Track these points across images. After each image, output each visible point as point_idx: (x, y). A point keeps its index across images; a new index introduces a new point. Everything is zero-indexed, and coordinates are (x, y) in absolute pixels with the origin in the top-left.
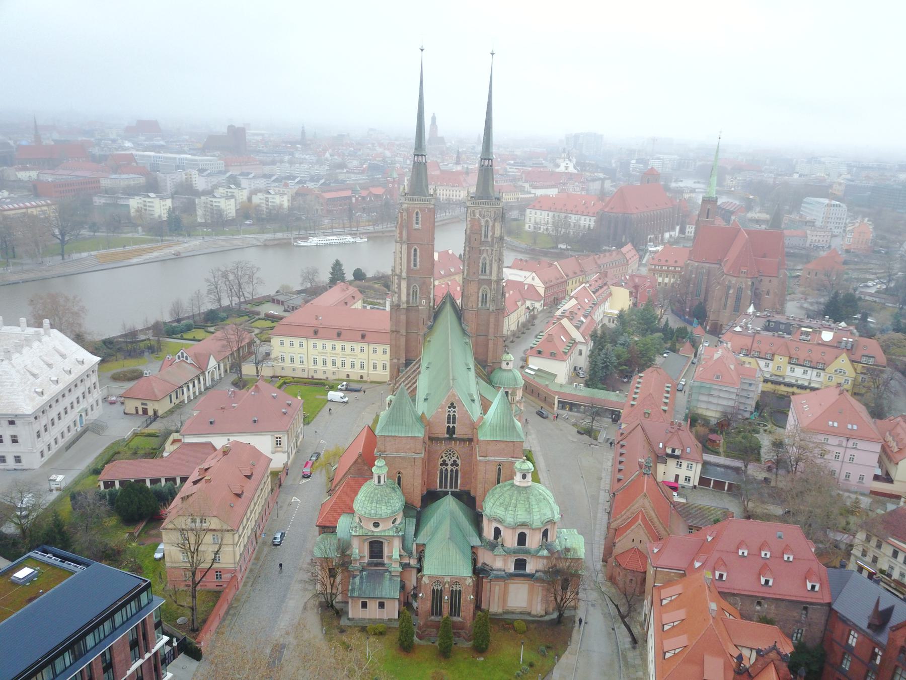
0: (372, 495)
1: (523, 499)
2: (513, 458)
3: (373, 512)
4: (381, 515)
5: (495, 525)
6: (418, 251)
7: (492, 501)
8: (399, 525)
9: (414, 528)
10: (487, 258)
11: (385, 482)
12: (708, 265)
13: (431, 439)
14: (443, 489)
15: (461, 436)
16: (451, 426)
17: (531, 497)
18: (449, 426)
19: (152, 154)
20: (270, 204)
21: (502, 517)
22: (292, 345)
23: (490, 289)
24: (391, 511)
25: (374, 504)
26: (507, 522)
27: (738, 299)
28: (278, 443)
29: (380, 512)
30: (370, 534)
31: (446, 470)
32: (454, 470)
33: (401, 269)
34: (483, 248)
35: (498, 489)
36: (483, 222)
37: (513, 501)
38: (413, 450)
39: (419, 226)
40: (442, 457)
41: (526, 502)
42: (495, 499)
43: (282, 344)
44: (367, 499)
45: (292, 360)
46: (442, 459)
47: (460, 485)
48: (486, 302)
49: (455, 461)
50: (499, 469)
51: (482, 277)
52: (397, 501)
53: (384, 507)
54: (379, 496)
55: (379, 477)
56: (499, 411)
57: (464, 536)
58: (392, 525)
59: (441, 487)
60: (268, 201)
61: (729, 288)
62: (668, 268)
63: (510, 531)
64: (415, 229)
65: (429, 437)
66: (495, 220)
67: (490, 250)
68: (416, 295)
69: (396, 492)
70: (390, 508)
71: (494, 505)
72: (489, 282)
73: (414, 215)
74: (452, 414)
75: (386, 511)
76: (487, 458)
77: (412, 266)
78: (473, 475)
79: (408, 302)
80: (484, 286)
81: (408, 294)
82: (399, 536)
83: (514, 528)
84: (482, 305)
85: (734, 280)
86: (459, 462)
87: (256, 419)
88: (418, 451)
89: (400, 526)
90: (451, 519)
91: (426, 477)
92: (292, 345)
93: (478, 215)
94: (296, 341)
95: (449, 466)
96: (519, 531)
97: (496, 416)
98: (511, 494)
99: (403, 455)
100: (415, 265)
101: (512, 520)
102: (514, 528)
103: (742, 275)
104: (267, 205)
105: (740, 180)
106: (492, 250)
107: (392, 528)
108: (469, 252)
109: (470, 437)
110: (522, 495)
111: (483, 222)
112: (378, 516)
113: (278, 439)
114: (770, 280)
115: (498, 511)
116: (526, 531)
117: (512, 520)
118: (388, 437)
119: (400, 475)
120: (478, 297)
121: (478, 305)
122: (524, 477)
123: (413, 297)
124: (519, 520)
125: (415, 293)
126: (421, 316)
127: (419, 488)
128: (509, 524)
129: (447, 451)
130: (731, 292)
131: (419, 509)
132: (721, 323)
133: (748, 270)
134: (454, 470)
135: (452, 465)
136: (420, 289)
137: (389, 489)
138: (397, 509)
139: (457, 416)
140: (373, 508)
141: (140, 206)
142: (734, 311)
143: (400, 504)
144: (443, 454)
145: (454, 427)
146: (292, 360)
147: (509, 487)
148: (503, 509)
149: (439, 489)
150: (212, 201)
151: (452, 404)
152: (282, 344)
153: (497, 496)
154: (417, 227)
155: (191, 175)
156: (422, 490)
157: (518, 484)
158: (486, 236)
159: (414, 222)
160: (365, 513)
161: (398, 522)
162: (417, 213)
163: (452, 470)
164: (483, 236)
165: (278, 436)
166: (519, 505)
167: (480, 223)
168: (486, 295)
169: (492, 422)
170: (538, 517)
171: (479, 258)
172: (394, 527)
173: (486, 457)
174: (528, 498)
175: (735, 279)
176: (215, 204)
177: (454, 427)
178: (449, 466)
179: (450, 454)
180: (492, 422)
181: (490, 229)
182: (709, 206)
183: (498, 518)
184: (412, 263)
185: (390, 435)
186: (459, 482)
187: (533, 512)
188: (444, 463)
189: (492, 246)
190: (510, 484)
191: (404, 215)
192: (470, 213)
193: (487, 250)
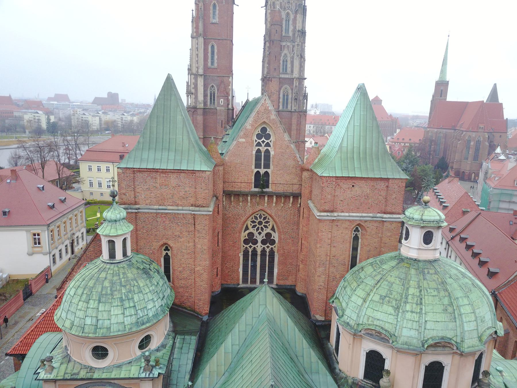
0: (91, 284)
1: (433, 285)
2: (385, 213)
3: (88, 321)
4: (109, 329)
5: (369, 345)
6: (216, 47)
7: (360, 292)
8: (158, 350)
9: (191, 355)
10: (288, 55)
11: (125, 254)
12: (445, 130)
13: (228, 194)
14: (249, 285)
15: (280, 189)
16: (262, 171)
17: (449, 281)
18: (258, 172)
19: (56, 103)
20: (124, 121)
21: (387, 327)
22: (99, 170)
23: (292, 90)
24: (134, 319)
25: (92, 304)
26: (401, 340)
27: (477, 150)
28: (37, 242)
29: (107, 323)
30: (83, 374)
31: (254, 252)
32: (268, 250)
33: (197, 68)
34: (284, 44)
35: (369, 270)
36: (284, 16)
37: (411, 291)
38: (192, 201)
39: (216, 20)
40: (247, 228)
41: (442, 293)
42: (368, 289)
43: (90, 169)
44: (80, 291)
45: (100, 185)
46: (247, 232)
47: (278, 274)
48: (287, 103)
49: (268, 235)
50: (356, 238)
51: (282, 76)
52: (150, 296)
53: (116, 311)
54: (107, 284)
55: (111, 243)
56: (357, 124)
57: (299, 373)
58: (139, 353)
59: (245, 281)
60: (122, 120)
61: (469, 141)
62: (405, 144)
63: (409, 361)
64: (213, 23)
65: (224, 192)
66: (296, 12)
67: (291, 46)
68: (214, 97)
69: (150, 277)
70: (133, 312)
71: (365, 301)
72: (291, 81)
73: (211, 8)
74: (263, 149)
75: (120, 319)
76: (335, 214)
77: (209, 64)
78: (301, 257)
79: (205, 103)
80: (285, 86)
81: (205, 96)
82: (153, 379)
83: (418, 354)
84: (283, 107)
85: (474, 135)
86: (275, 236)
87: (7, 210)
88: (200, 202)
89: (159, 354)
90: (271, 336)
91: (219, 261)
92: (99, 170)
93: (278, 7)
94: (103, 166)
95: (259, 244)
96: (428, 359)
97: (351, 133)
98: (403, 276)
99: (171, 209)
100: (212, 63)
101: (413, 333)
102: (418, 354)
103: (481, 130)
104: (122, 122)
105: (418, 123)
106: (293, 46)
107: (138, 360)
108: (269, 47)
109: (295, 189)
110: (428, 277)
111: (284, 16)
112: (100, 333)
113: (37, 237)
114: (500, 136)
115: (378, 315)
116: (446, 360)
117: (413, 333)
118: (140, 170)
119: (169, 253)
120: (279, 98)
121: (279, 106)
122: (428, 238)
123: (211, 99)
124: (429, 334)
125: (212, 96)
126: (218, 118)
127: (205, 276)
128: (406, 344)
129: (256, 218)
130: (472, 143)
131: (205, 318)
132: (463, 171)
133: (484, 126)
134: (268, 250)
135: (264, 242)
136: (218, 90)
137: (135, 271)
138: (151, 315)
139: (272, 153)
140: (90, 311)
141: (31, 119)
142: (474, 160)
143: (158, 304)
144: (249, 222)
145: (267, 173)
146: (100, 185)
147: (393, 263)
148: (391, 310)
149: (242, 285)
150: (83, 117)
151: (264, 130)
152: (90, 169)
153: (371, 282)
154: (214, 21)
155: (76, 111)
156: (212, 286)
157: (413, 254)
158: (287, 30)
159: (211, 15)
160: (72, 324)
161: (154, 345)
162: (214, 5)
163: (263, 251)
164: (284, 31)
165: (36, 232)
166: (427, 300)
167: (281, 16)
168: (287, 96)
169: (345, 144)
170: (472, 326)
171: (280, 54)
172: (143, 355)
173: (332, 211)
174: (443, 283)
175: (474, 133)
176: (84, 119)
177: (267, 173)
178: (259, 244)
179: (260, 223)
180: (345, 144)
181: (291, 22)
182: (442, 88)
183: (378, 329)
184: (210, 60)
185: (144, 166)
186: (276, 271)
187: (460, 315)
188: (251, 239)
189: (293, 41)
190: (392, 258)
191: (200, 5)
192: (270, 5)
193: (288, 46)
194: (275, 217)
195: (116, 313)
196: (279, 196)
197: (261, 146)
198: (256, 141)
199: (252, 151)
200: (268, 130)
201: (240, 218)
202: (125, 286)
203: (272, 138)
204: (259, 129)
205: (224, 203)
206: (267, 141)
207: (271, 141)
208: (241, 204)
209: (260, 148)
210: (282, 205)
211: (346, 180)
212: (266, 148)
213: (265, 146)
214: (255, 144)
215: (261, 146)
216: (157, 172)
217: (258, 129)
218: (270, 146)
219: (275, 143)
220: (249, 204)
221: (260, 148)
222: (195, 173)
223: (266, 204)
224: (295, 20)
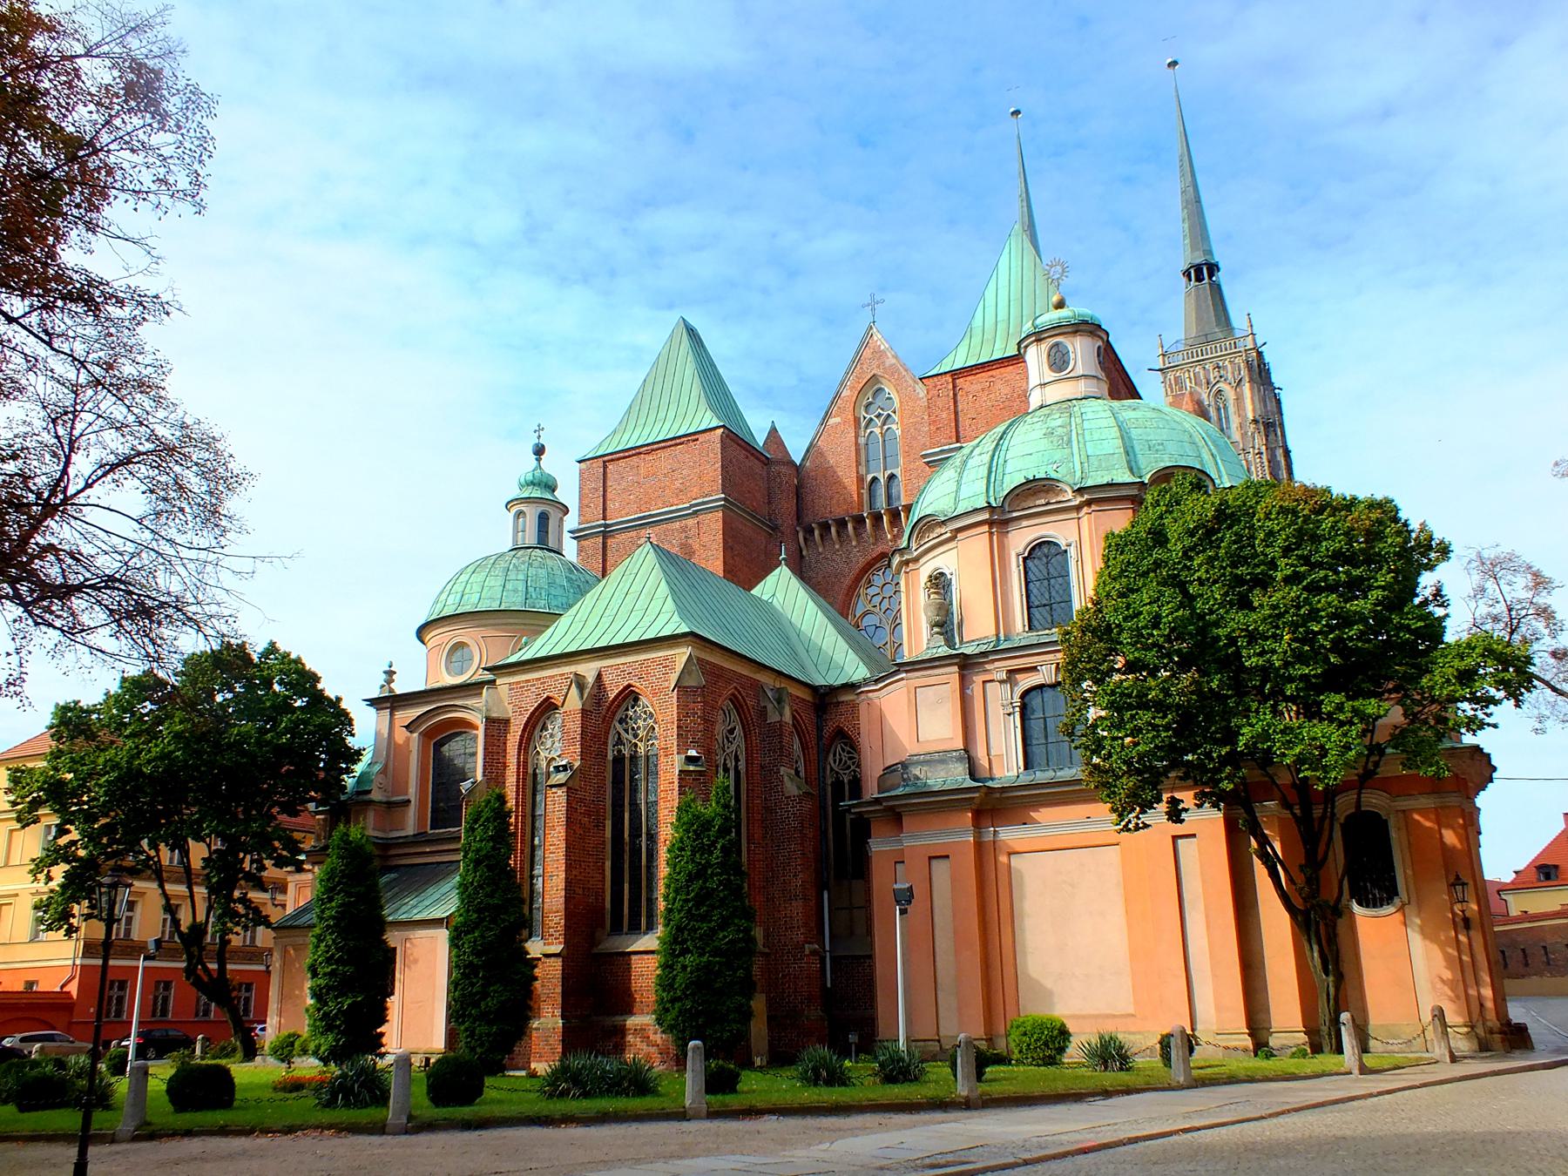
139: (898, 433)
195: (492, 584)
198: (865, 418)
201: (839, 580)
202: (518, 558)
203: (897, 405)
205: (804, 553)
206: (886, 413)
208: (837, 547)
216: (640, 453)
218: (894, 422)
220: (854, 543)
222: (697, 440)
224: (1239, 399)
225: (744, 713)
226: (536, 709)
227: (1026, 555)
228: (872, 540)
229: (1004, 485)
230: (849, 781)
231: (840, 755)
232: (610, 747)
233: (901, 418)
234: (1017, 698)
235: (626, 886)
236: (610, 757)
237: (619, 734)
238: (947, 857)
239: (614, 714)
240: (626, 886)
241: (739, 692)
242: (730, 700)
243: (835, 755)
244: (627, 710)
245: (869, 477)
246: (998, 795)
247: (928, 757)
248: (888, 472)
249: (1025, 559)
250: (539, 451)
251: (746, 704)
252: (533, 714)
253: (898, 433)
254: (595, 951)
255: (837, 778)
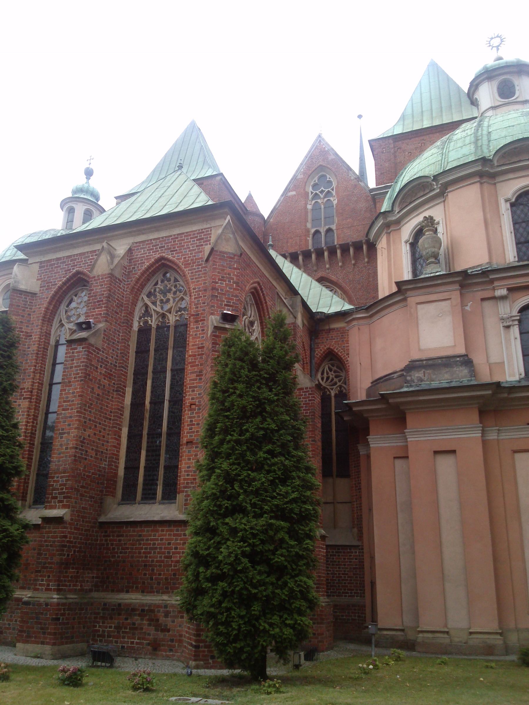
194: (343, 285)
196: (345, 249)
197: (320, 198)
198: (312, 193)
199: (306, 204)
200: (328, 176)
203: (334, 185)
204: (316, 179)
207: (333, 190)
209: (319, 201)
210: (353, 262)
211: (411, 139)
212: (326, 199)
213: (325, 197)
214: (310, 196)
215: (320, 198)
217: (314, 178)
219: (337, 187)
221: (319, 201)
223: (327, 266)
225: (263, 310)
226: (64, 284)
227: (513, 200)
228: (315, 268)
229: (491, 148)
230: (336, 396)
231: (327, 373)
232: (136, 318)
233: (337, 193)
234: (515, 312)
235: (143, 453)
236: (136, 327)
237: (147, 306)
238: (454, 452)
239: (143, 286)
240: (143, 453)
241: (261, 289)
242: (252, 293)
243: (322, 374)
244: (156, 284)
245: (313, 231)
246: (506, 395)
247: (430, 362)
248: (327, 227)
249: (512, 205)
250: (89, 173)
251: (266, 303)
252: (60, 288)
253: (335, 202)
254: (102, 519)
255: (324, 393)
